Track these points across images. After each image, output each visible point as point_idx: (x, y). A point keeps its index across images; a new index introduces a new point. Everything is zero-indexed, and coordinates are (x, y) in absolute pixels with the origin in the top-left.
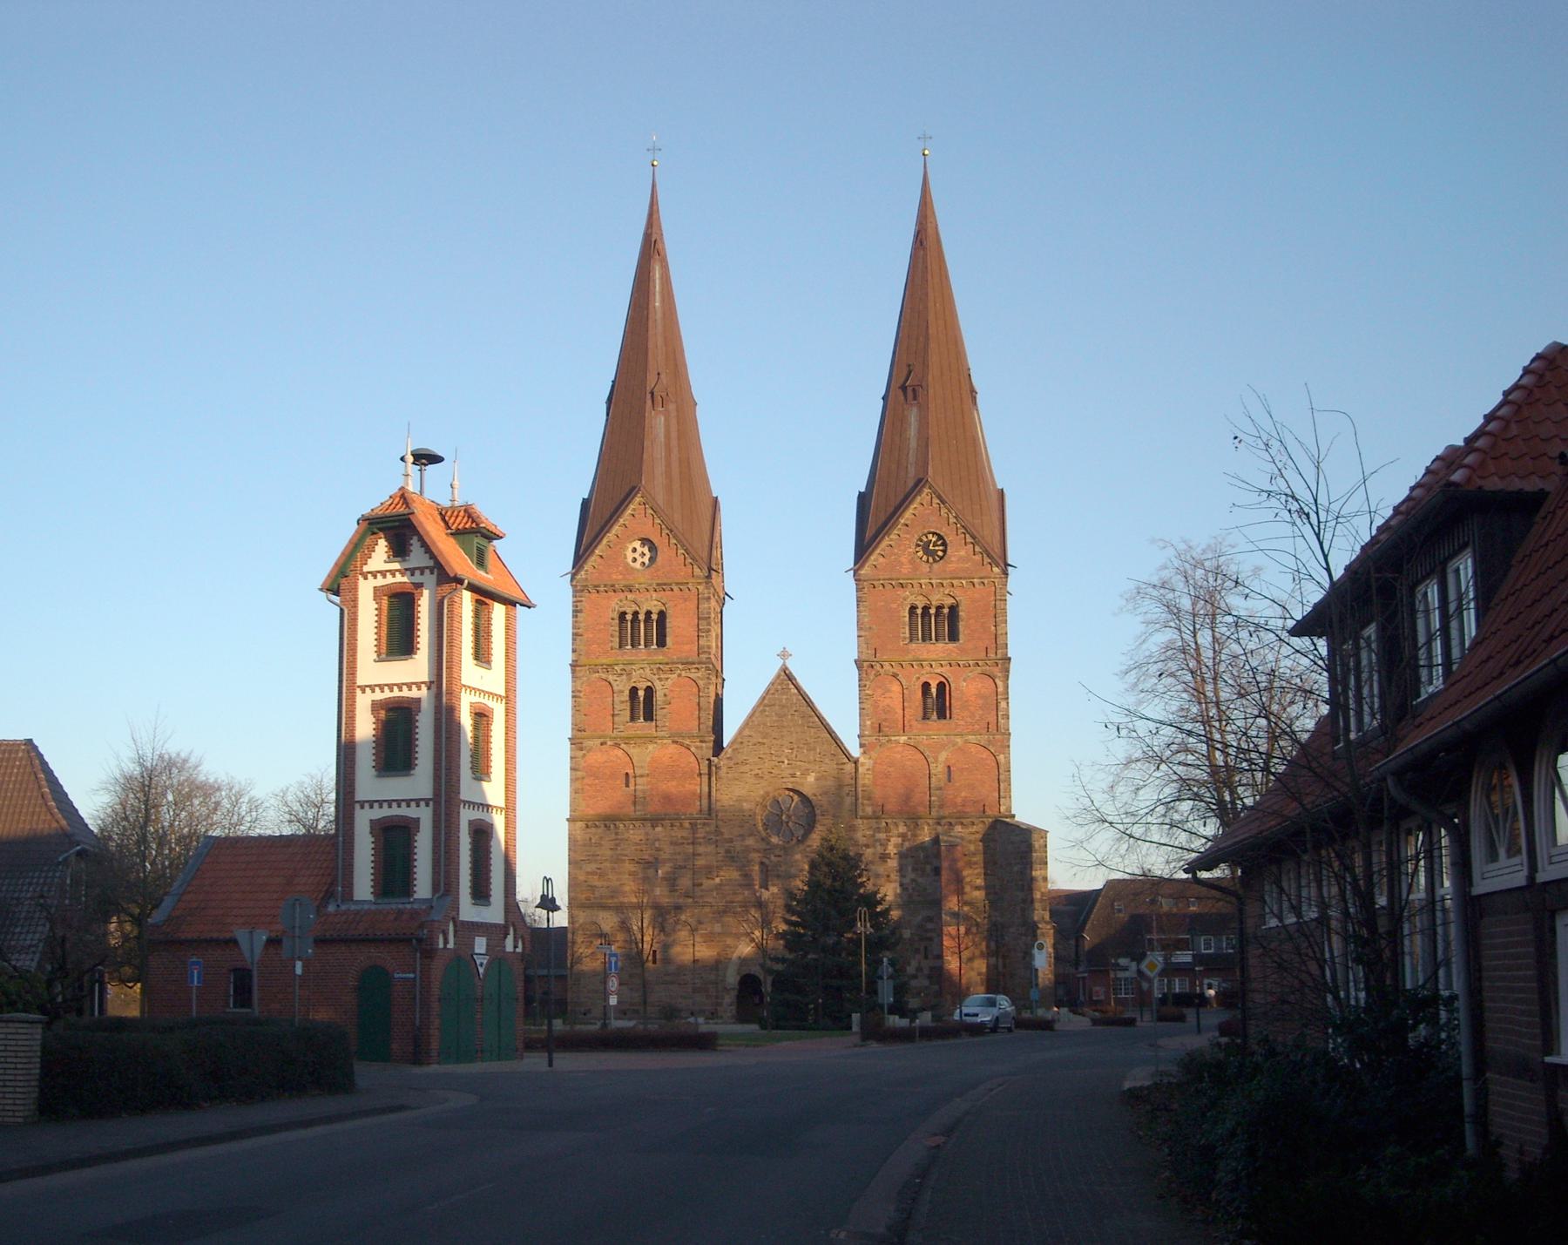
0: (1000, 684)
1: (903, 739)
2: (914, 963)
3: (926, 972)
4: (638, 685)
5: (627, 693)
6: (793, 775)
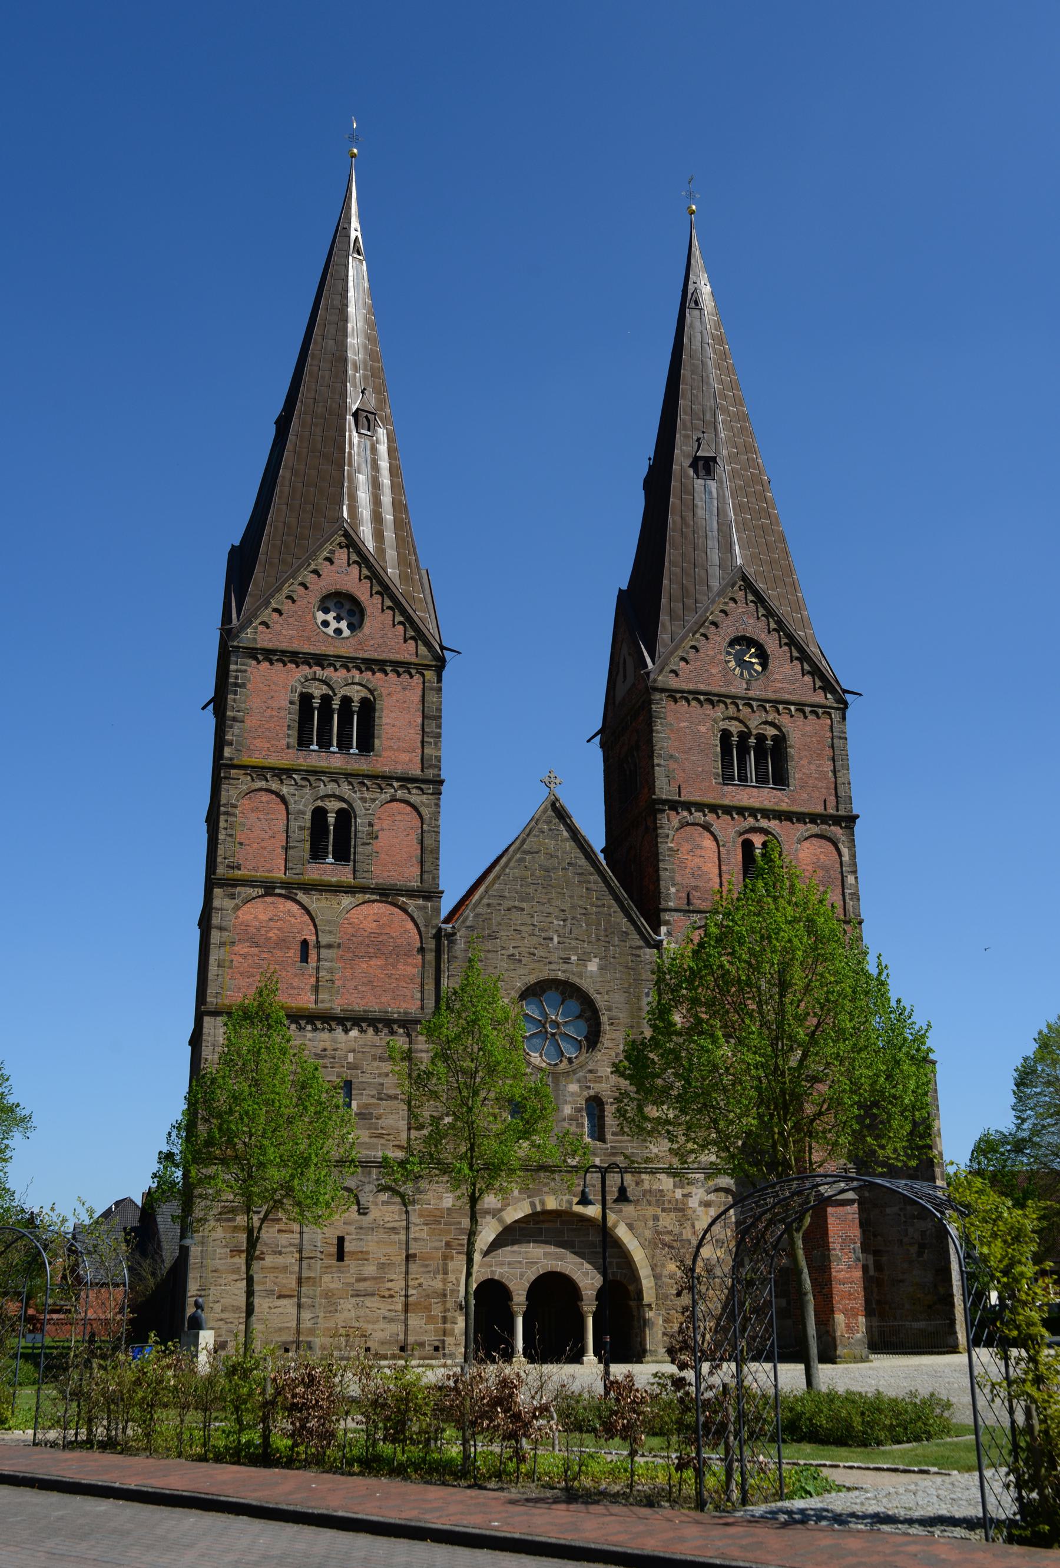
0: (845, 851)
5: (308, 816)
6: (566, 960)
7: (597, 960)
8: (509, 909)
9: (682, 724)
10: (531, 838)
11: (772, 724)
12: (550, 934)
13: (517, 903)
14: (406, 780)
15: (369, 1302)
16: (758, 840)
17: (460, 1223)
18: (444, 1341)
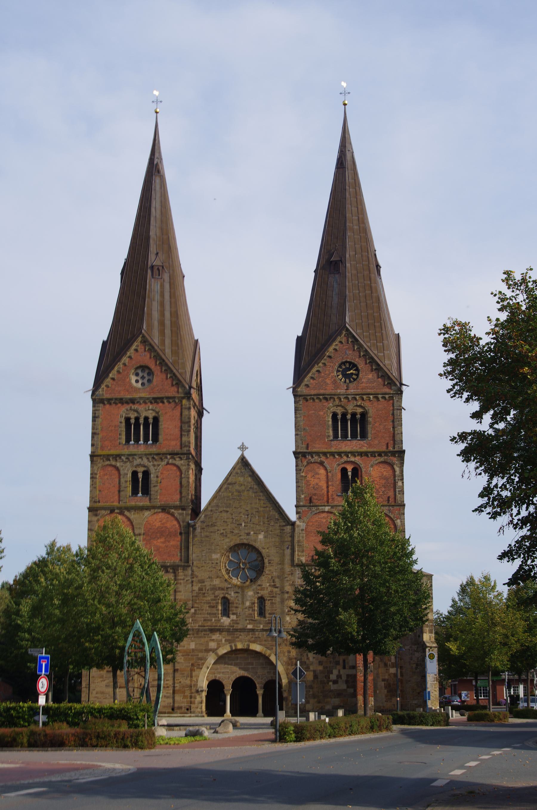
0: (397, 469)
1: (327, 509)
2: (335, 672)
3: (344, 678)
6: (248, 534)
7: (263, 533)
8: (221, 512)
9: (311, 412)
11: (360, 406)
13: (225, 509)
14: (173, 454)
16: (350, 468)
17: (198, 655)
18: (190, 707)
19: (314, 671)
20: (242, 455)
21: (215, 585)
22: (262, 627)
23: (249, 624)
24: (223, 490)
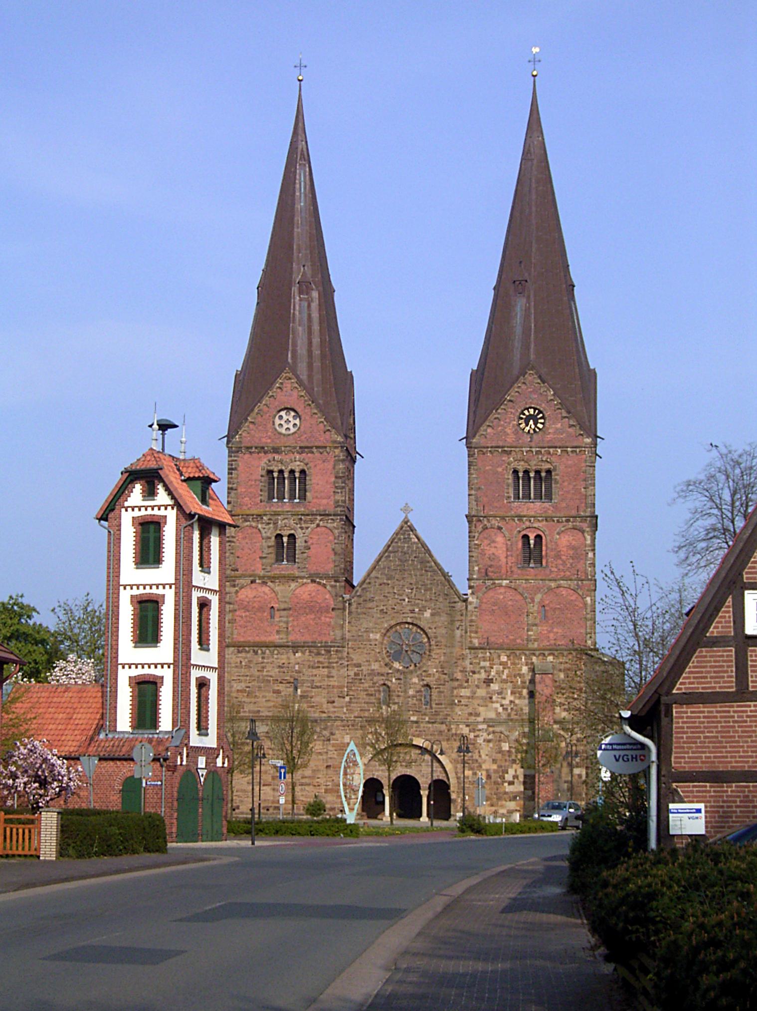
1: (505, 582)
2: (511, 772)
4: (283, 533)
6: (412, 611)
7: (430, 611)
10: (393, 544)
12: (404, 597)
15: (307, 788)
19: (487, 771)
20: (406, 517)
21: (373, 670)
22: (427, 719)
23: (413, 715)
24: (383, 559)
